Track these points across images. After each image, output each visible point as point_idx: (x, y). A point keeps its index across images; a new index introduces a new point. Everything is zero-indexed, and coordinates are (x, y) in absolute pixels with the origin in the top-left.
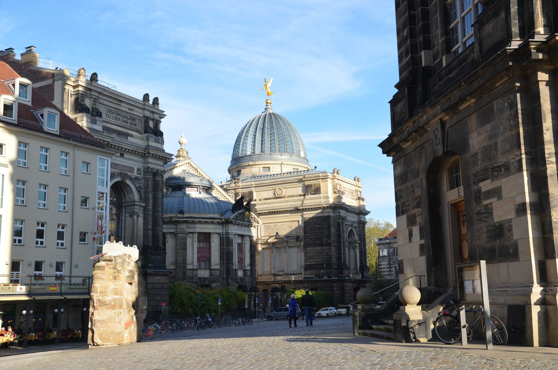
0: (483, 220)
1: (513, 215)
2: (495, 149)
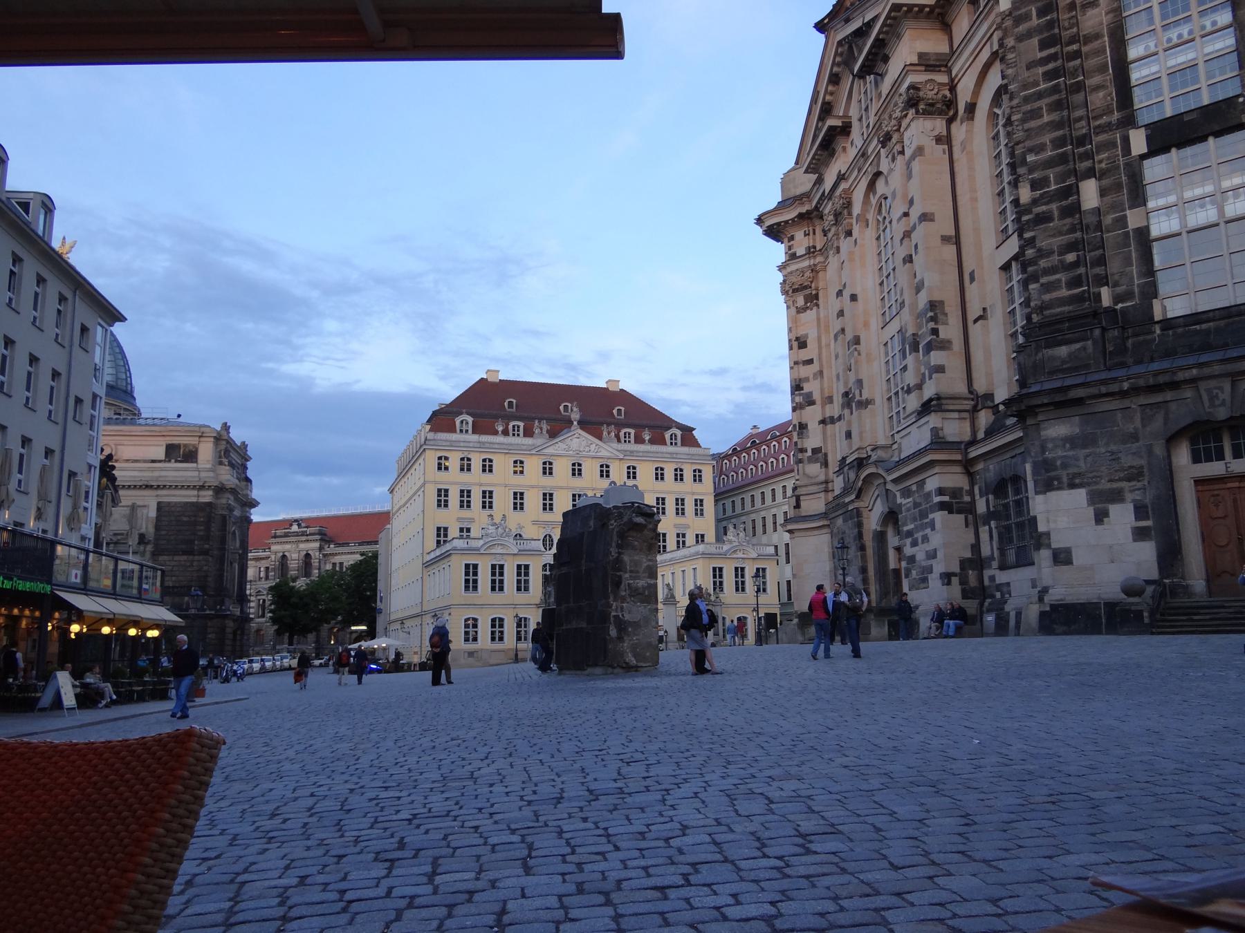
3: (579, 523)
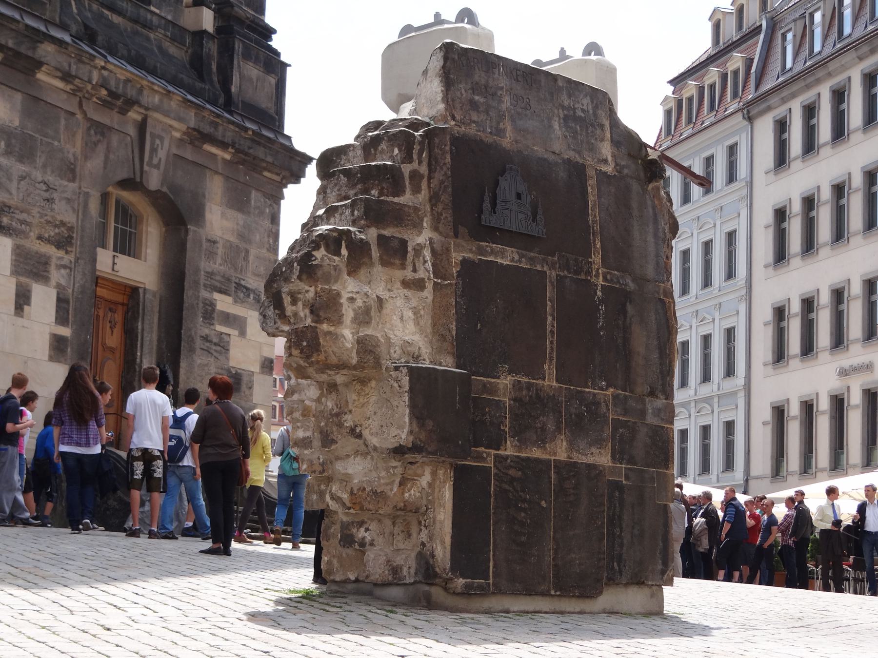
0: (212, 354)
1: (256, 368)
2: (244, 259)
3: (556, 126)
